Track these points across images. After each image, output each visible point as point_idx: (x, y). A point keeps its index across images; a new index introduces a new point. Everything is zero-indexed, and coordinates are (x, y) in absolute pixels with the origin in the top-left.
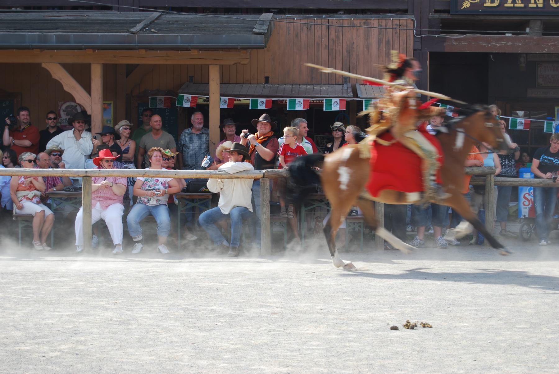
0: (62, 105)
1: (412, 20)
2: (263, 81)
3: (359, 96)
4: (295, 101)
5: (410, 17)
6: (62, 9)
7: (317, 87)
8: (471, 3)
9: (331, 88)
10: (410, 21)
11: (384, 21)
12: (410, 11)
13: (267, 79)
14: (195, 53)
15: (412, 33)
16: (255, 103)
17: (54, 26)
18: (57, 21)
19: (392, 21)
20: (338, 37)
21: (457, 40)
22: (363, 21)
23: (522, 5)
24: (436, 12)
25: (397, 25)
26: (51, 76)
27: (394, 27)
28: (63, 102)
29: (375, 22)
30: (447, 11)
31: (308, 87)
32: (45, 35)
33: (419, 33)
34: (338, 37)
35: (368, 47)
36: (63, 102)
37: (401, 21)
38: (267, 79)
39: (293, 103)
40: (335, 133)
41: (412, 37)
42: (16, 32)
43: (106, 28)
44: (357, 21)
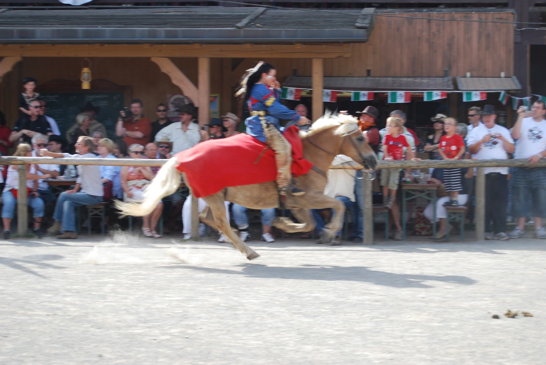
0: (171, 97)
1: (513, 14)
2: (365, 74)
3: (460, 88)
4: (395, 93)
5: (510, 11)
7: (418, 80)
9: (432, 81)
13: (369, 72)
14: (299, 47)
15: (513, 26)
16: (357, 95)
17: (163, 21)
19: (492, 15)
20: (439, 31)
24: (537, 5)
27: (495, 20)
29: (475, 15)
31: (410, 79)
32: (154, 30)
33: (519, 26)
34: (439, 31)
35: (469, 41)
39: (394, 96)
43: (212, 23)
44: (458, 14)
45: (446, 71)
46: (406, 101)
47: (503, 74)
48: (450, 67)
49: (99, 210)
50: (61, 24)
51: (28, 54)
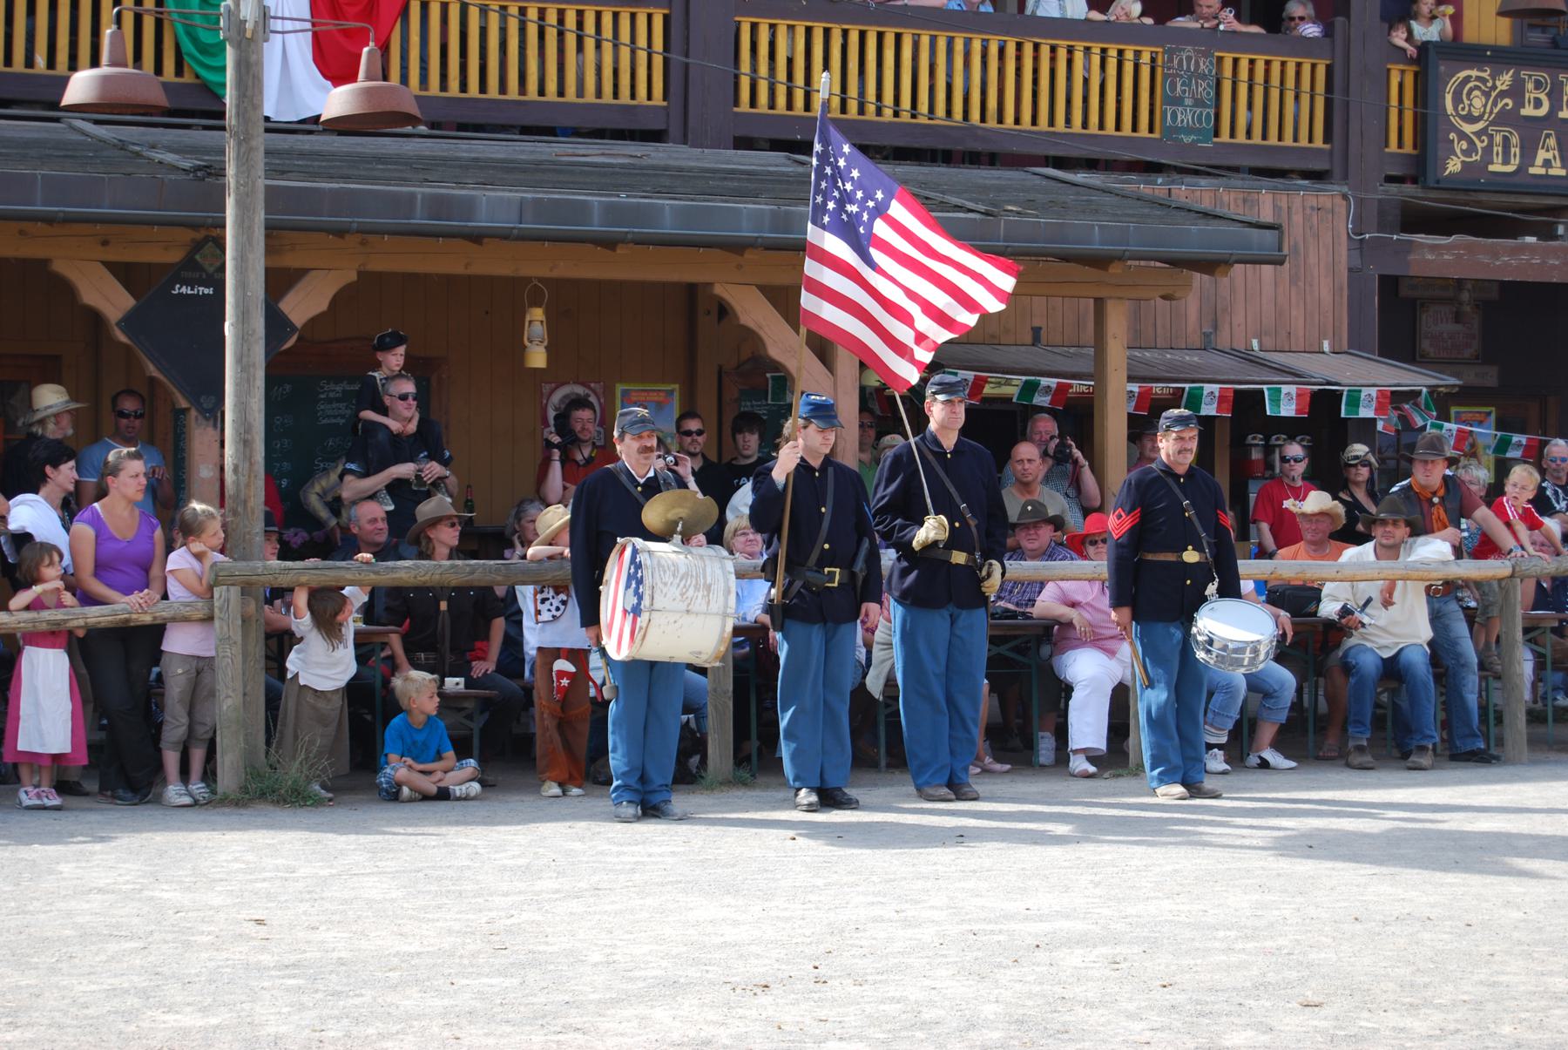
0: (552, 392)
1: (1345, 197)
2: (1028, 339)
4: (1279, 390)
5: (1336, 189)
6: (555, 135)
8: (1463, 162)
10: (1339, 201)
11: (1284, 198)
12: (1337, 171)
13: (1036, 332)
17: (607, 178)
18: (617, 170)
21: (1433, 248)
22: (1241, 196)
23: (1563, 173)
24: (1390, 179)
25: (1312, 208)
26: (737, 318)
28: (553, 385)
30: (1414, 181)
32: (787, 213)
36: (553, 385)
37: (1321, 199)
38: (1036, 332)
40: (1353, 470)
41: (1344, 237)
42: (708, 201)
45: (1206, 335)
46: (1298, 411)
47: (1326, 346)
48: (1216, 327)
49: (464, 713)
50: (480, 180)
51: (378, 265)
